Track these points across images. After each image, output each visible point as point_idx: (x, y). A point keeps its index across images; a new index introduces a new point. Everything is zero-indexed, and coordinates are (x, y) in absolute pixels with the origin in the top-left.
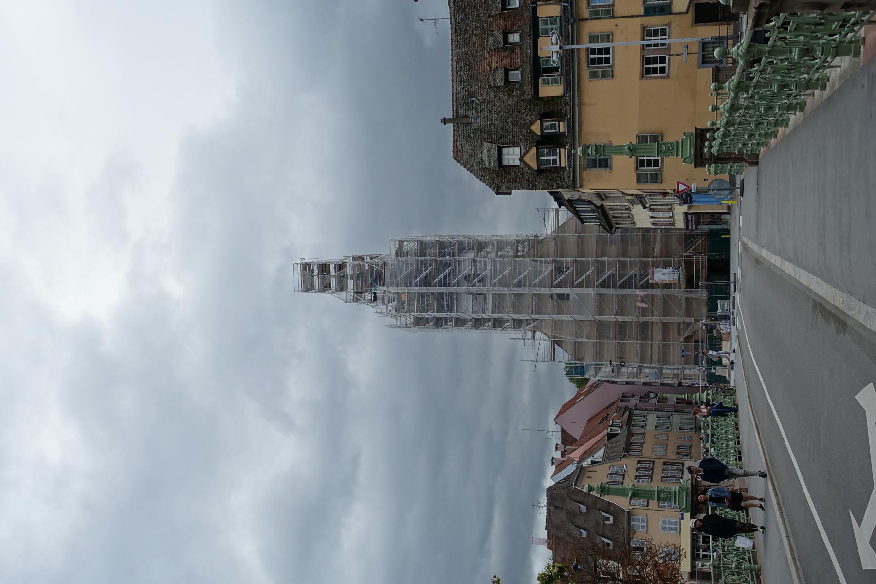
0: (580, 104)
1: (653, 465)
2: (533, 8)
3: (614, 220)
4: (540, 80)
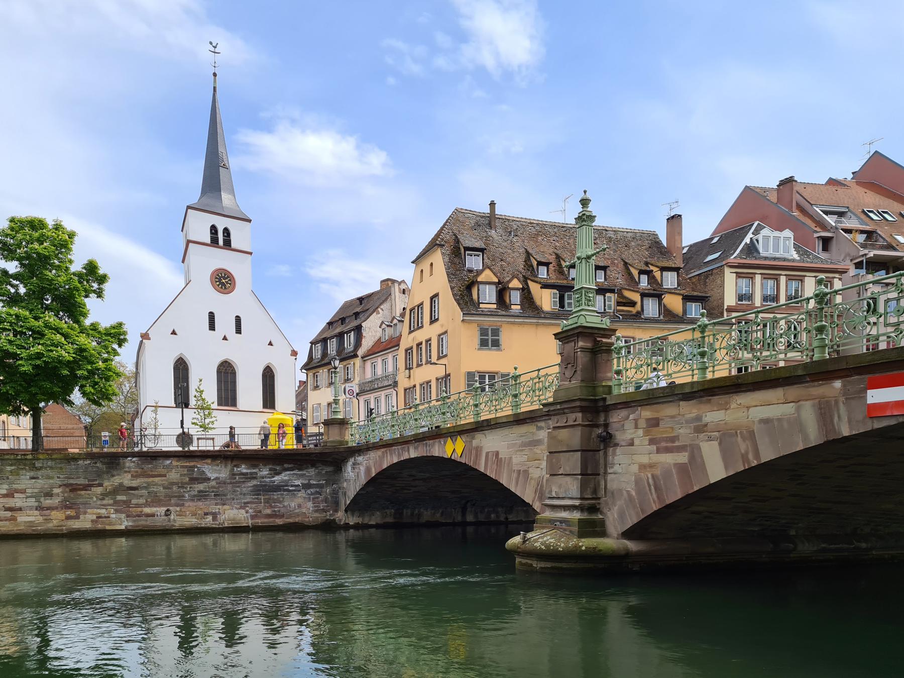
0: (537, 324)
2: (614, 290)
4: (555, 291)
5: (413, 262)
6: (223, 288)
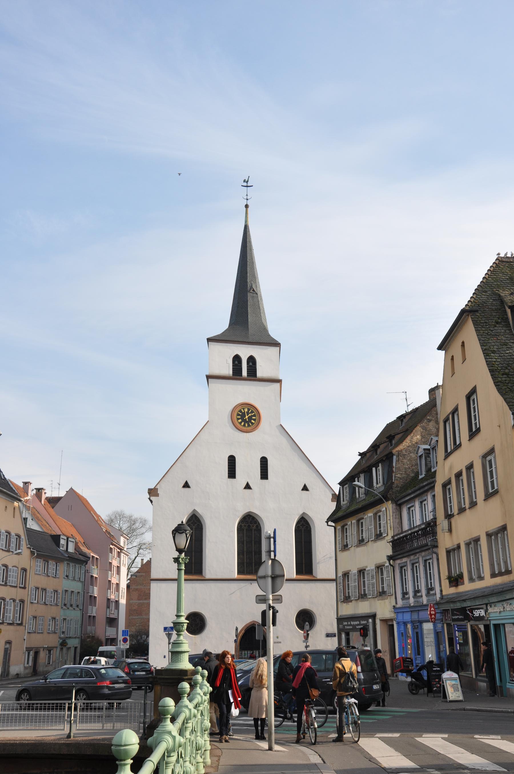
1: (20, 587)
3: (354, 521)
5: (440, 348)
6: (246, 425)
